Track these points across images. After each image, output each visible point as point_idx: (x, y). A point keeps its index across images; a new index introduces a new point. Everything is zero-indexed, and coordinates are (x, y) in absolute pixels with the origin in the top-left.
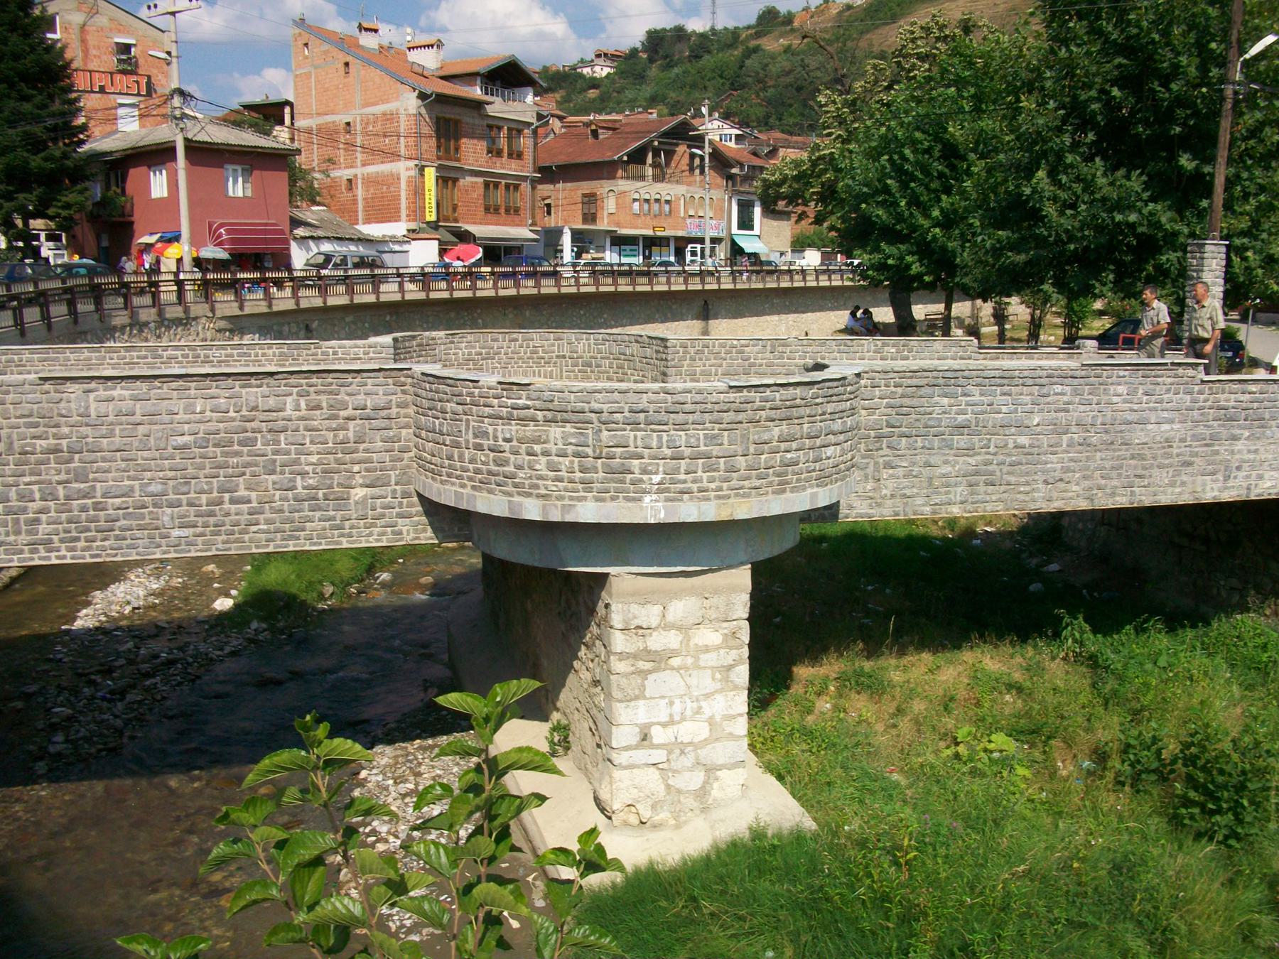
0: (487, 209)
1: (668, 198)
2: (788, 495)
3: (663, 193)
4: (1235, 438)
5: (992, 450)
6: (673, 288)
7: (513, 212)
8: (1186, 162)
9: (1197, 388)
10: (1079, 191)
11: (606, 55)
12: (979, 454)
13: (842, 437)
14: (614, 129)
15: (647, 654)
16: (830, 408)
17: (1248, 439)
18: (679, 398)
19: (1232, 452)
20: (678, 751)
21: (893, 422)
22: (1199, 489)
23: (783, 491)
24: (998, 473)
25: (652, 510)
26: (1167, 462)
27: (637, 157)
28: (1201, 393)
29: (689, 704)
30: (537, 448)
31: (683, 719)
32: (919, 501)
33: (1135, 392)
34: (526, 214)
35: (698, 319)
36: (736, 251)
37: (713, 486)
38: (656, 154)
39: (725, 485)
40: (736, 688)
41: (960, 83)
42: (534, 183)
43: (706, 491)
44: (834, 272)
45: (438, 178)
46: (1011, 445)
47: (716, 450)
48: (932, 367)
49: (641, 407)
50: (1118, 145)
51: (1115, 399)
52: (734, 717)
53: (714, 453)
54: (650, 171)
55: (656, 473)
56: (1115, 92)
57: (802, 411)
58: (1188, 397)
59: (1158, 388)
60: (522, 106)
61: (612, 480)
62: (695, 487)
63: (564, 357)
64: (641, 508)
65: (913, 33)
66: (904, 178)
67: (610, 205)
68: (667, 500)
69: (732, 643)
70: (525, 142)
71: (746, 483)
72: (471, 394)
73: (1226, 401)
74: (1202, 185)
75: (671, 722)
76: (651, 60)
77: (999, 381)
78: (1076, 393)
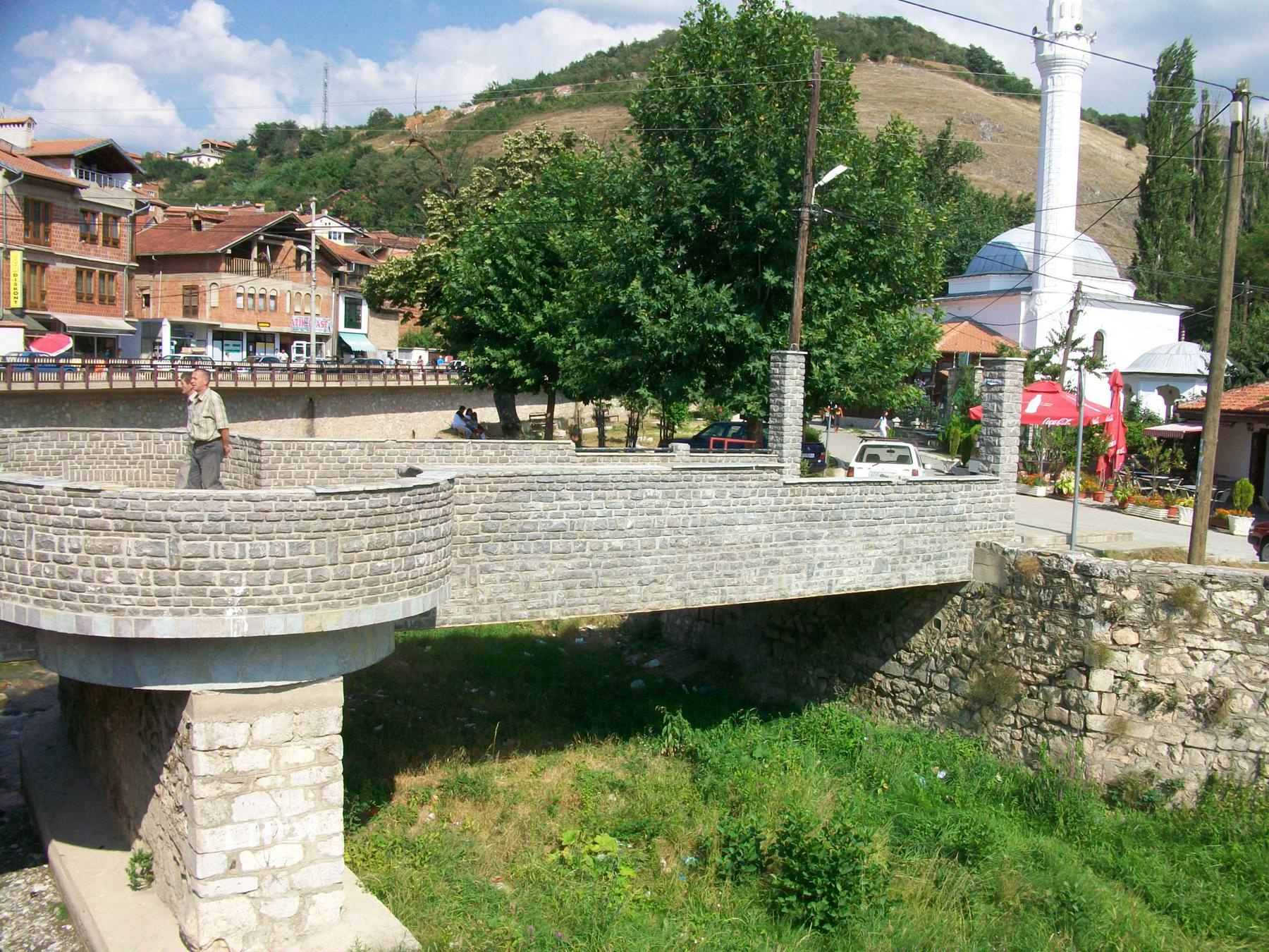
0: (79, 298)
1: (274, 294)
2: (379, 604)
3: (269, 289)
4: (816, 537)
5: (587, 553)
6: (277, 385)
7: (107, 301)
8: (770, 276)
9: (780, 490)
10: (672, 302)
11: (213, 146)
13: (434, 544)
14: (218, 222)
15: (234, 776)
16: (422, 514)
18: (262, 505)
20: (269, 878)
21: (489, 526)
22: (785, 586)
23: (375, 600)
24: (594, 576)
25: (234, 623)
27: (242, 250)
28: (784, 495)
29: (281, 827)
30: (108, 559)
31: (274, 843)
32: (517, 605)
33: (723, 495)
34: (122, 304)
35: (302, 416)
36: (343, 348)
37: (300, 597)
38: (262, 248)
39: (313, 596)
40: (330, 806)
41: (562, 193)
42: (131, 272)
43: (293, 602)
44: (441, 372)
45: (24, 263)
46: (606, 548)
47: (302, 560)
48: (527, 472)
49: (221, 515)
50: (707, 258)
51: (705, 502)
52: (330, 837)
53: (301, 563)
54: (254, 266)
55: (239, 585)
56: (705, 209)
57: (393, 518)
58: (772, 499)
59: (744, 491)
60: (120, 193)
61: (188, 593)
62: (280, 598)
63: (151, 457)
64: (223, 622)
65: (517, 143)
66: (507, 283)
67: (213, 298)
68: (251, 612)
69: (325, 759)
70: (122, 231)
71: (335, 593)
72: (33, 501)
73: (807, 502)
74: (782, 299)
75: (262, 846)
76: (261, 154)
77: (593, 485)
78: (667, 496)
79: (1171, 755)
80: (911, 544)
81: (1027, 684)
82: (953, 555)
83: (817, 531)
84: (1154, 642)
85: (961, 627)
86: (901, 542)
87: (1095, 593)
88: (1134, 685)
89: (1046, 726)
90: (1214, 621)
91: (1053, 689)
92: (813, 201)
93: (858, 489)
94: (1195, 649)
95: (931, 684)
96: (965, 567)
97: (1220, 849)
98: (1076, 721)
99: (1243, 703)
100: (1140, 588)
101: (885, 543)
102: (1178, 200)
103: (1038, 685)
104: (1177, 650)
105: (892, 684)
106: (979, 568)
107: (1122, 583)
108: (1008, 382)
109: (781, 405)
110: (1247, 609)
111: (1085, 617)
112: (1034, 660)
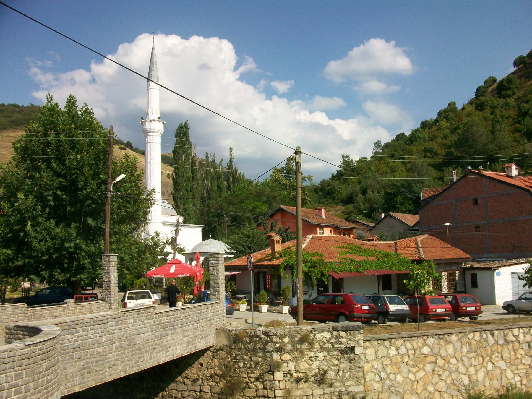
4: (167, 335)
5: (89, 356)
8: (90, 221)
9: (154, 316)
10: (45, 234)
12: (84, 359)
17: (171, 335)
19: (167, 341)
24: (92, 367)
26: (148, 349)
28: (156, 318)
46: (96, 353)
47: (20, 382)
50: (59, 214)
51: (130, 325)
53: (20, 384)
56: (59, 192)
58: (152, 321)
59: (143, 318)
74: (101, 232)
77: (89, 324)
80: (197, 333)
81: (247, 383)
82: (210, 335)
83: (167, 332)
84: (297, 357)
85: (213, 364)
87: (272, 342)
88: (291, 375)
90: (317, 346)
91: (258, 383)
92: (112, 189)
93: (179, 312)
94: (311, 357)
95: (201, 391)
96: (213, 339)
99: (331, 374)
100: (289, 337)
101: (189, 333)
102: (188, 184)
105: (181, 394)
106: (218, 339)
107: (282, 336)
108: (220, 261)
109: (109, 278)
110: (328, 339)
111: (269, 352)
112: (248, 373)
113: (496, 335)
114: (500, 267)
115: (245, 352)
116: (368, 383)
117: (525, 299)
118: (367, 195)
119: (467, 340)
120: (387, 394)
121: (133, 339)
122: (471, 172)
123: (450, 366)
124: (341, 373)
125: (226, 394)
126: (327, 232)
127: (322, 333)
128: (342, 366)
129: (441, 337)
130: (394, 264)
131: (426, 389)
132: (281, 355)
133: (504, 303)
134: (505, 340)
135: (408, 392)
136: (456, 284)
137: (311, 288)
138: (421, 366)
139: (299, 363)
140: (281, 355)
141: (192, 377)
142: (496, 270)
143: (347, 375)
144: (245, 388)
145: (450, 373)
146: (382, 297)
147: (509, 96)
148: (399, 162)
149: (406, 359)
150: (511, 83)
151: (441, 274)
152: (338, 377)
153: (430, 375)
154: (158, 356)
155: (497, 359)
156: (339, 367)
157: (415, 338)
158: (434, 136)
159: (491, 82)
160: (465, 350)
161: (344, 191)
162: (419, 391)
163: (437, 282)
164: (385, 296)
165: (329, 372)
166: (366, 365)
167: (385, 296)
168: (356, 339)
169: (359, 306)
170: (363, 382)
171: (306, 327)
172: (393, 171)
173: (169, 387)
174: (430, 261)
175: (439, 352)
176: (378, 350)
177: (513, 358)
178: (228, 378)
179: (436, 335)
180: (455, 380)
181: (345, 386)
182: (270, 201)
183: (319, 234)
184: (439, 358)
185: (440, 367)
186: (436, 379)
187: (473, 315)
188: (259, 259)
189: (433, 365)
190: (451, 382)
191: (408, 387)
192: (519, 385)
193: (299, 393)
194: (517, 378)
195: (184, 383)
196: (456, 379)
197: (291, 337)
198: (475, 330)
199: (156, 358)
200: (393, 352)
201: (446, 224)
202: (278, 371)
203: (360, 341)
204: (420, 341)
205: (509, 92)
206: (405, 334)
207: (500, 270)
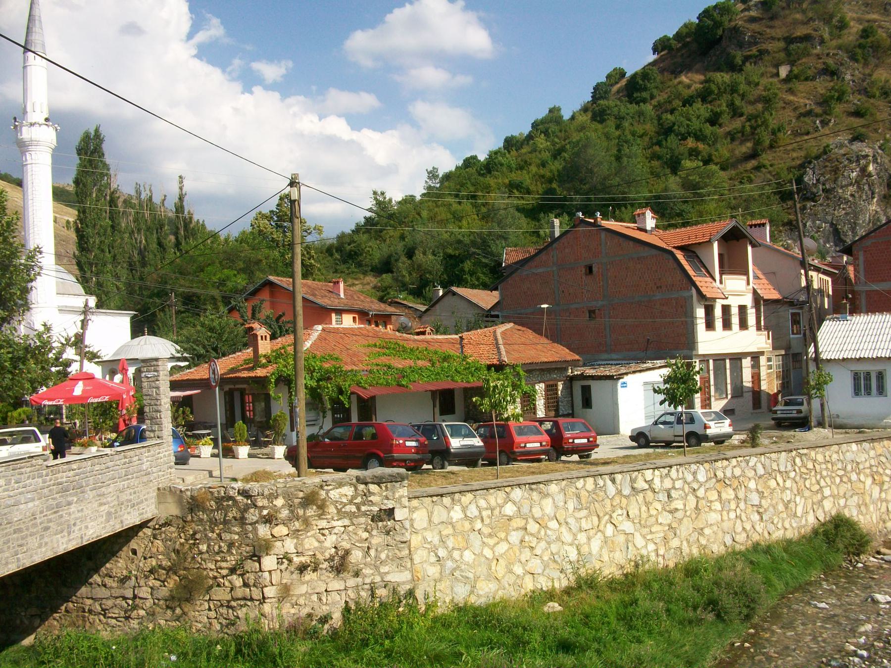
4: (69, 504)
9: (44, 472)
19: (70, 514)
22: (56, 546)
59: (22, 476)
79: (320, 599)
80: (124, 497)
81: (215, 578)
82: (146, 500)
83: (70, 499)
84: (298, 531)
85: (154, 550)
86: (118, 497)
88: (290, 561)
89: (233, 604)
90: (332, 510)
91: (235, 577)
93: (89, 463)
95: (135, 597)
96: (153, 506)
97: (378, 648)
98: (256, 593)
99: (356, 556)
100: (284, 498)
101: (109, 499)
102: (103, 238)
103: (223, 577)
104: (312, 533)
105: (100, 605)
106: (162, 506)
107: (272, 497)
108: (161, 373)
110: (350, 498)
111: (250, 524)
112: (217, 561)
113: (618, 482)
114: (627, 374)
115: (210, 527)
116: (418, 567)
117: (664, 423)
118: (414, 258)
119: (574, 490)
120: (448, 583)
121: (5, 514)
122: (582, 221)
123: (549, 532)
124: (372, 552)
125: (179, 600)
126: (348, 321)
127: (339, 488)
128: (375, 541)
129: (534, 487)
130: (459, 372)
131: (511, 572)
132: (271, 528)
133: (633, 431)
134: (633, 488)
135: (482, 577)
136: (557, 402)
137: (321, 414)
138: (502, 535)
139: (303, 540)
140: (271, 528)
141: (119, 575)
142: (619, 378)
143: (383, 556)
144: (211, 587)
145: (549, 543)
146: (438, 427)
147: (644, 101)
148: (467, 205)
149: (478, 525)
150: (649, 80)
151: (533, 385)
152: (369, 559)
153: (516, 549)
154: (55, 541)
155: (620, 518)
156: (370, 543)
157: (492, 491)
158: (526, 162)
159: (618, 76)
160: (571, 505)
161: (376, 251)
162: (500, 576)
163: (528, 400)
164: (444, 424)
165: (353, 552)
166: (414, 537)
167: (444, 424)
168: (397, 495)
169: (401, 442)
170: (409, 565)
171: (312, 479)
172: (458, 218)
173: (78, 594)
174: (517, 366)
175: (531, 511)
176: (432, 513)
177: (644, 515)
178: (182, 572)
179: (525, 484)
180: (557, 554)
181: (380, 574)
182: (249, 269)
183: (334, 325)
184: (530, 520)
185: (531, 534)
186: (527, 554)
187: (584, 452)
188: (233, 369)
189: (521, 533)
190: (550, 559)
191: (482, 570)
192: (653, 557)
193: (303, 589)
194: (651, 547)
195: (105, 586)
196: (558, 553)
197: (288, 496)
198: (586, 474)
199: (50, 544)
200: (457, 514)
201: (543, 306)
202: (267, 554)
203: (403, 499)
204: (501, 495)
205: (645, 95)
206: (476, 485)
207: (626, 379)
